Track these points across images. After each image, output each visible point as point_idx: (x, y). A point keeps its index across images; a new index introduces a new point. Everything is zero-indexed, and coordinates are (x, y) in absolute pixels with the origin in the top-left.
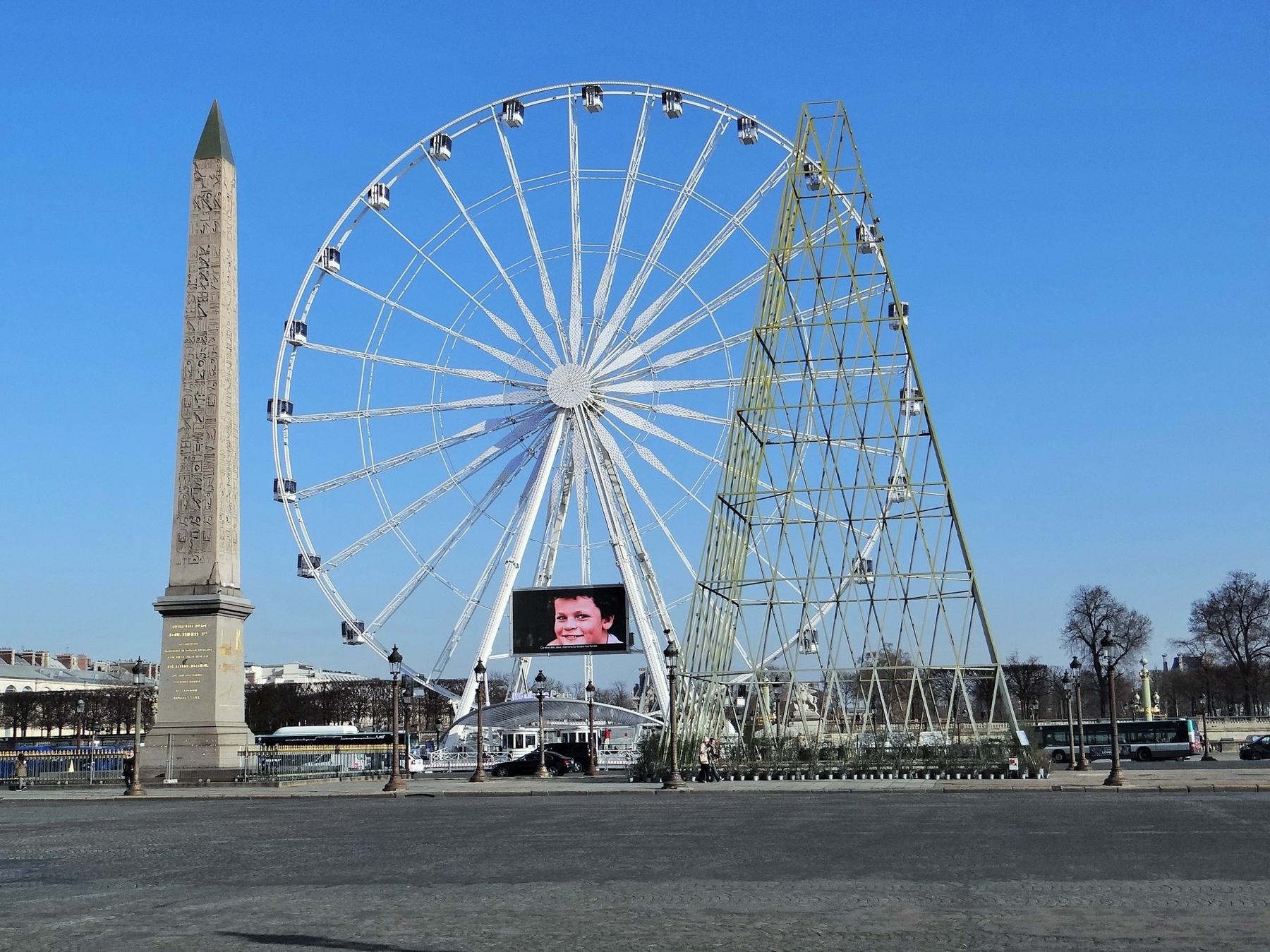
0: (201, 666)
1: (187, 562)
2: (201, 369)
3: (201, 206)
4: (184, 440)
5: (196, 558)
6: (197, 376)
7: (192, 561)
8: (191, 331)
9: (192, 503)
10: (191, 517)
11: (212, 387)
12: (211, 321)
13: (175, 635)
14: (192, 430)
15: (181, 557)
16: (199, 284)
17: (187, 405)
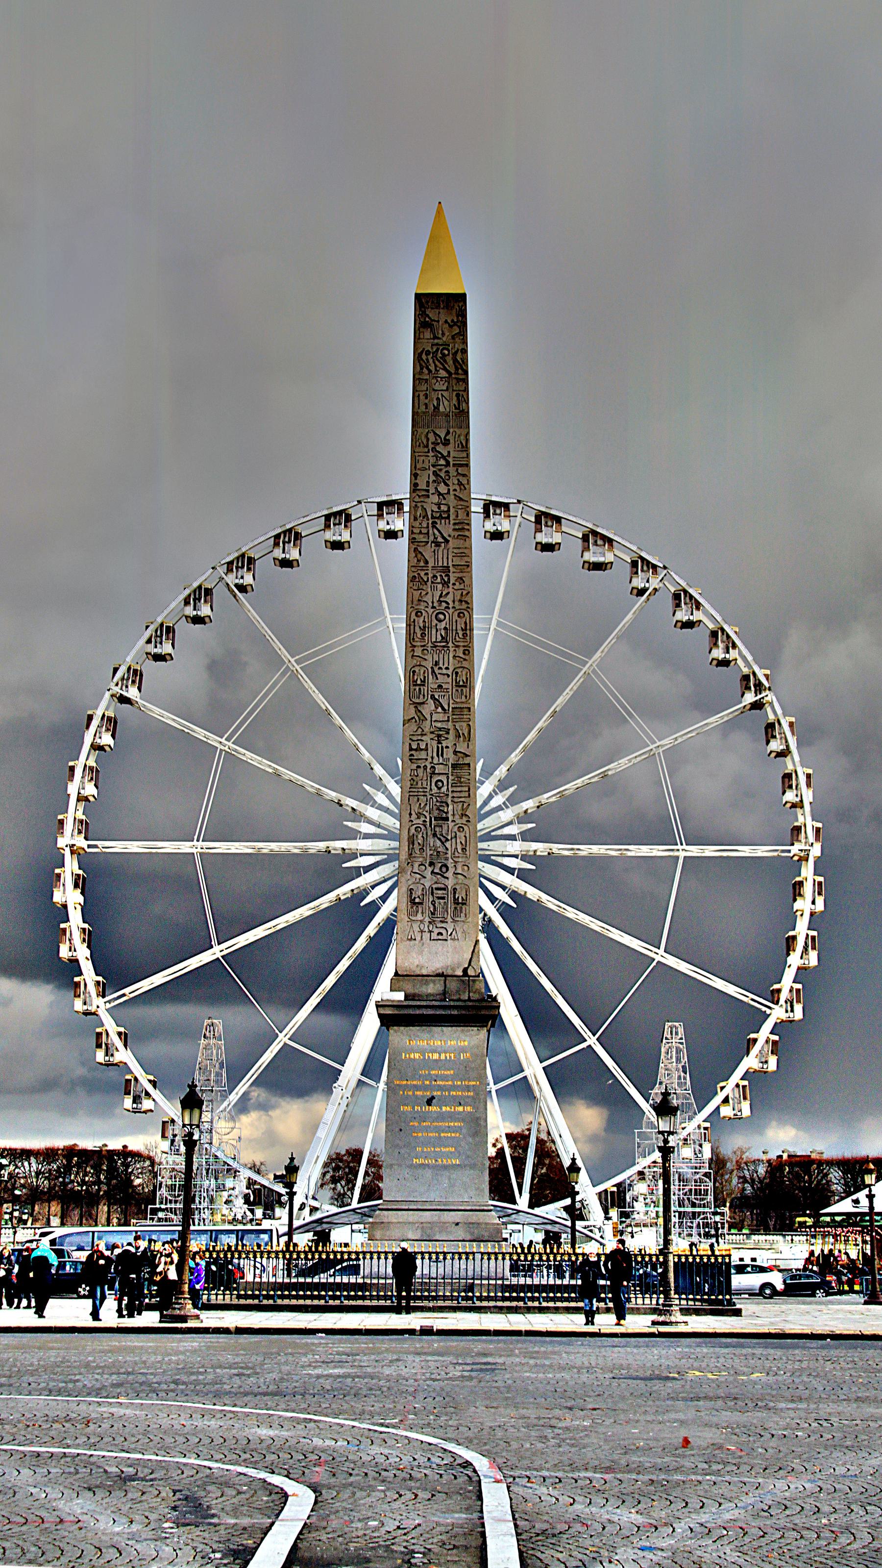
0: (461, 1109)
1: (426, 935)
2: (443, 625)
3: (432, 368)
4: (415, 738)
5: (444, 932)
6: (435, 636)
7: (434, 936)
8: (422, 564)
9: (431, 840)
10: (432, 864)
11: (461, 655)
12: (455, 551)
13: (412, 1056)
14: (428, 722)
15: (416, 927)
16: (432, 490)
17: (419, 682)
